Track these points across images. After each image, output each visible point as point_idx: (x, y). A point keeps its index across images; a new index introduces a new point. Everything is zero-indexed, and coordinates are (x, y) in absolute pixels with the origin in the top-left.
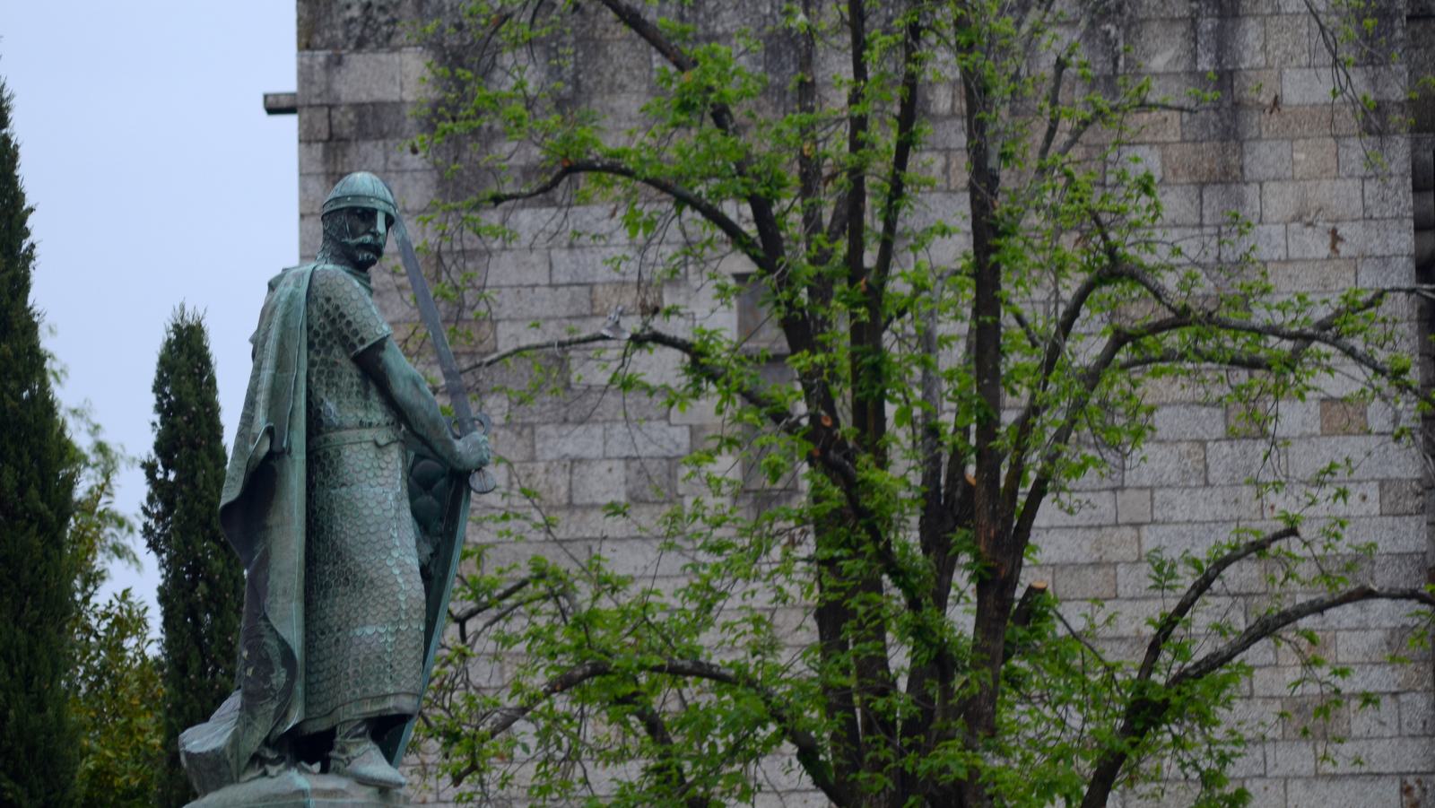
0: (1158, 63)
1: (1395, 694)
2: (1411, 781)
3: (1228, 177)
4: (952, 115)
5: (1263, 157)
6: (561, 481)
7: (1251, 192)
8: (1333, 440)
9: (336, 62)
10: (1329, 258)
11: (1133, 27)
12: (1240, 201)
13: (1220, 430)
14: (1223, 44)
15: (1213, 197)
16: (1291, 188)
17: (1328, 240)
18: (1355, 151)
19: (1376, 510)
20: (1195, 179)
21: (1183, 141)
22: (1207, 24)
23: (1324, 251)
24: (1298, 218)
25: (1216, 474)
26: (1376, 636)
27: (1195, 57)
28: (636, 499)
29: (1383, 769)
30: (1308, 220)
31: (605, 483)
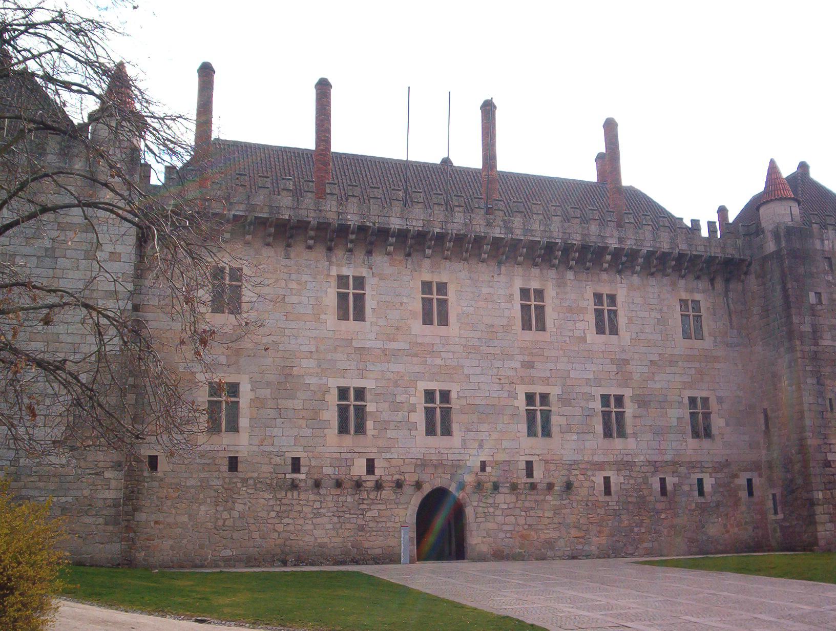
25: (81, 268)
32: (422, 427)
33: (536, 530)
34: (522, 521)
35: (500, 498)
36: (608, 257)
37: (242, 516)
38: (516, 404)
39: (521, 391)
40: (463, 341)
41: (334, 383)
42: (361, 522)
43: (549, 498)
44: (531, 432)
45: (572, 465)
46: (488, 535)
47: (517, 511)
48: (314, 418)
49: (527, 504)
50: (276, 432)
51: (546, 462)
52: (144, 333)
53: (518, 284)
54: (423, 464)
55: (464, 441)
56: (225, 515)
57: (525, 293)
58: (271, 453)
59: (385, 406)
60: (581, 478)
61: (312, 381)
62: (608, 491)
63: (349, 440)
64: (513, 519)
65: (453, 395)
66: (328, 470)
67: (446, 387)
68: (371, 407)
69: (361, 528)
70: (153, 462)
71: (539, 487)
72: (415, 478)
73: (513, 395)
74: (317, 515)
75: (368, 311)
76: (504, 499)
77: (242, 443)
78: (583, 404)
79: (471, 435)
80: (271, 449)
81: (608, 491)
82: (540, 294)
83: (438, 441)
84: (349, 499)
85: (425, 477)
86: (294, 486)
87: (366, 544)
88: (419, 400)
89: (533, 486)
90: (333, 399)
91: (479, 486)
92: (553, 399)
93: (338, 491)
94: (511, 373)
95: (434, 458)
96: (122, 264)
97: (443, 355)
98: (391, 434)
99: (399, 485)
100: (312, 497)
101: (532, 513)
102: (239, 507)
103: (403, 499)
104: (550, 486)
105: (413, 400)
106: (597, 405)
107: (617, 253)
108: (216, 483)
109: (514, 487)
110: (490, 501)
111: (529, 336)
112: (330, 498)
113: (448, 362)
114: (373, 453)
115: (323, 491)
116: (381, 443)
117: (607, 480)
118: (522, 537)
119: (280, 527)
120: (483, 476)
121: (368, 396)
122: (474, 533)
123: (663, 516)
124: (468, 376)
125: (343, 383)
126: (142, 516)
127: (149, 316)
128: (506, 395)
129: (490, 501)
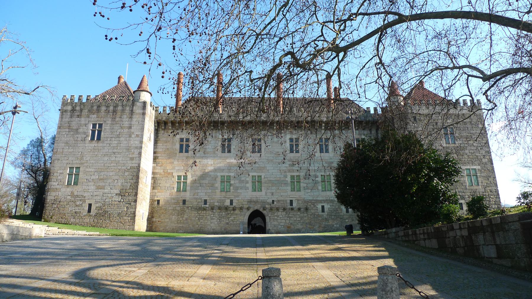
3: (131, 118)
5: (134, 116)
18: (141, 116)
31: (79, 139)
32: (250, 188)
33: (293, 225)
34: (288, 222)
35: (279, 213)
36: (323, 125)
37: (186, 219)
38: (287, 179)
39: (289, 175)
40: (267, 158)
41: (219, 174)
42: (227, 221)
43: (299, 213)
44: (293, 190)
45: (310, 201)
46: (275, 226)
47: (286, 218)
48: (212, 186)
49: (290, 215)
50: (199, 191)
51: (298, 200)
52: (157, 160)
53: (288, 136)
54: (250, 202)
55: (266, 193)
56: (181, 219)
57: (291, 140)
58: (197, 198)
59: (237, 181)
60: (312, 206)
61: (212, 174)
62: (323, 211)
63: (224, 194)
64: (284, 221)
65: (263, 177)
66: (216, 204)
67: (259, 174)
68: (232, 182)
69: (227, 224)
70: (158, 201)
71: (295, 209)
72: (247, 206)
73: (286, 177)
74: (212, 219)
75: (232, 150)
76: (280, 213)
77: (187, 195)
78: (314, 179)
79: (269, 191)
80: (197, 197)
81: (323, 211)
82: (297, 140)
83: (257, 194)
84: (224, 213)
85: (251, 206)
86: (204, 209)
87: (229, 229)
88: (249, 179)
89: (292, 209)
90: (219, 179)
91: (271, 209)
92: (302, 177)
93: (220, 211)
94: (286, 168)
95: (255, 199)
97: (259, 163)
98: (239, 191)
99: (241, 209)
100: (211, 213)
101: (292, 219)
102: (186, 216)
103: (243, 213)
104: (299, 209)
105: (247, 179)
106: (319, 179)
107: (327, 123)
108: (178, 208)
109: (284, 209)
110: (276, 214)
111: (292, 155)
112: (216, 213)
113: (261, 166)
114: (232, 197)
115: (214, 211)
116: (235, 194)
117: (323, 207)
118: (288, 227)
119: (199, 223)
120: (273, 205)
121: (231, 179)
122: (269, 226)
123: (347, 221)
124: (268, 170)
125: (222, 174)
126: (154, 219)
127: (159, 155)
128: (283, 176)
129: (276, 214)
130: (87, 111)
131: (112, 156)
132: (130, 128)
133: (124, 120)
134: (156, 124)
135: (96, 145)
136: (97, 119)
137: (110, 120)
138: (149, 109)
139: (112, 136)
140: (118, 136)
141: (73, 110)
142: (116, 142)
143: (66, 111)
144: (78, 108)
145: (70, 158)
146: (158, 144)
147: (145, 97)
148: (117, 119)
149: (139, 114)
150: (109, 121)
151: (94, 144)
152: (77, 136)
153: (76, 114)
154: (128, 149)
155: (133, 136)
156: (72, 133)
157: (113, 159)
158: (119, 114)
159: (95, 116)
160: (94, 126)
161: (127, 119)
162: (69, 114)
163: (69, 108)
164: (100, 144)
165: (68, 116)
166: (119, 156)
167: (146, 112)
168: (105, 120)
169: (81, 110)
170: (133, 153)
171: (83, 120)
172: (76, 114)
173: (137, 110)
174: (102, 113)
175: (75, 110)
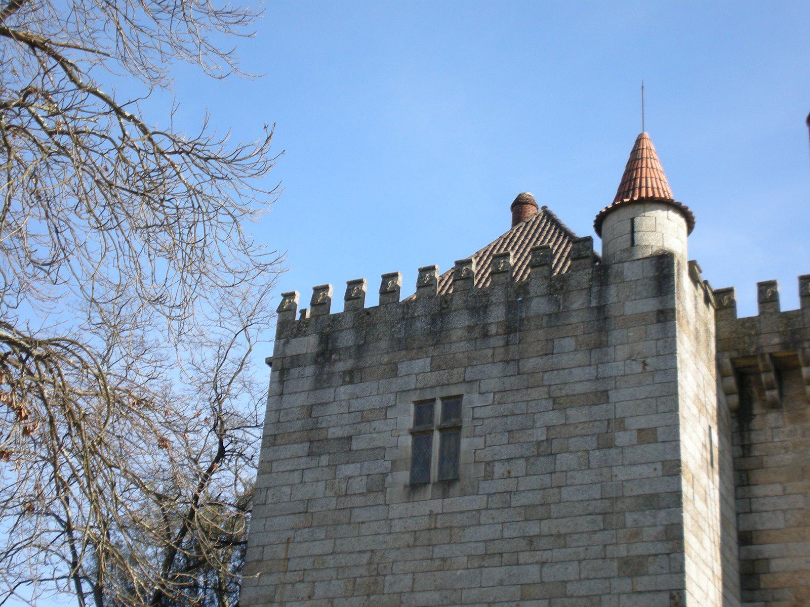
0: (575, 306)
1: (668, 554)
2: (674, 593)
4: (497, 334)
5: (616, 336)
6: (343, 486)
7: (611, 350)
8: (643, 446)
9: (287, 342)
10: (642, 373)
11: (567, 293)
12: (606, 354)
13: (595, 445)
14: (601, 295)
15: (595, 354)
16: (627, 347)
17: (642, 365)
19: (660, 473)
20: (588, 348)
21: (584, 334)
22: (595, 289)
23: (640, 370)
24: (629, 358)
25: (593, 464)
26: (660, 528)
27: (590, 302)
28: (370, 491)
29: (662, 588)
30: (633, 358)
31: (358, 485)
96: (660, 446)
130: (383, 344)
131: (524, 557)
132: (603, 396)
133: (564, 360)
134: (731, 382)
135: (436, 505)
136: (432, 378)
137: (496, 370)
138: (689, 301)
139: (513, 450)
140: (546, 450)
141: (325, 354)
142: (533, 482)
143: (296, 361)
144: (347, 339)
145: (320, 590)
146: (759, 491)
147: (663, 231)
148: (530, 364)
149: (641, 319)
150: (492, 376)
151: (429, 503)
152: (349, 470)
153: (340, 367)
154: (608, 514)
155: (622, 438)
156: (324, 460)
157: (533, 573)
158: (536, 337)
159: (423, 363)
160: (423, 407)
161: (580, 357)
162: (309, 370)
163: (308, 344)
164: (457, 502)
165: (307, 384)
166: (558, 554)
167: (678, 306)
168: (470, 374)
169: (360, 350)
170: (636, 535)
171: (371, 394)
172: (340, 367)
173: (629, 301)
174: (458, 344)
175: (334, 350)
